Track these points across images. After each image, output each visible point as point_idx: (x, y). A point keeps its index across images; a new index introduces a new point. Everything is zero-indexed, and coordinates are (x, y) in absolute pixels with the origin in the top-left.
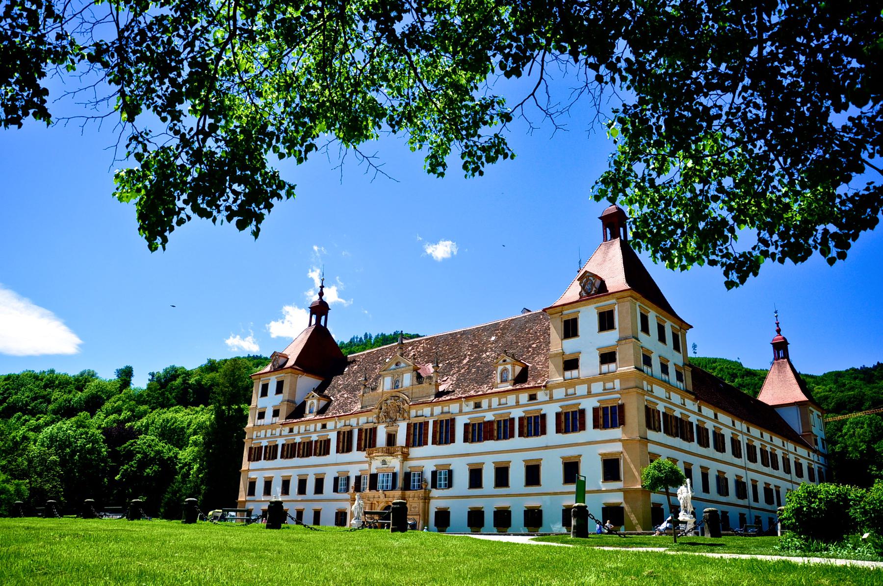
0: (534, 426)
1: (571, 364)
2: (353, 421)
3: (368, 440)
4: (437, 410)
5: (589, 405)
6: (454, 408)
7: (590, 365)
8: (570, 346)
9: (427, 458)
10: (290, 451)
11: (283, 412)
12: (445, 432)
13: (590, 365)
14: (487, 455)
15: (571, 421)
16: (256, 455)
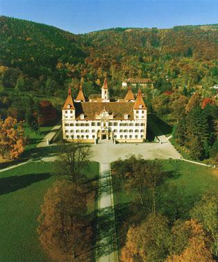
0: (131, 125)
1: (137, 117)
2: (94, 121)
3: (99, 124)
4: (114, 121)
5: (140, 123)
6: (117, 121)
7: (140, 118)
8: (137, 115)
9: (113, 128)
10: (77, 125)
11: (74, 117)
12: (115, 124)
13: (140, 118)
14: (123, 128)
15: (137, 125)
16: (66, 125)
